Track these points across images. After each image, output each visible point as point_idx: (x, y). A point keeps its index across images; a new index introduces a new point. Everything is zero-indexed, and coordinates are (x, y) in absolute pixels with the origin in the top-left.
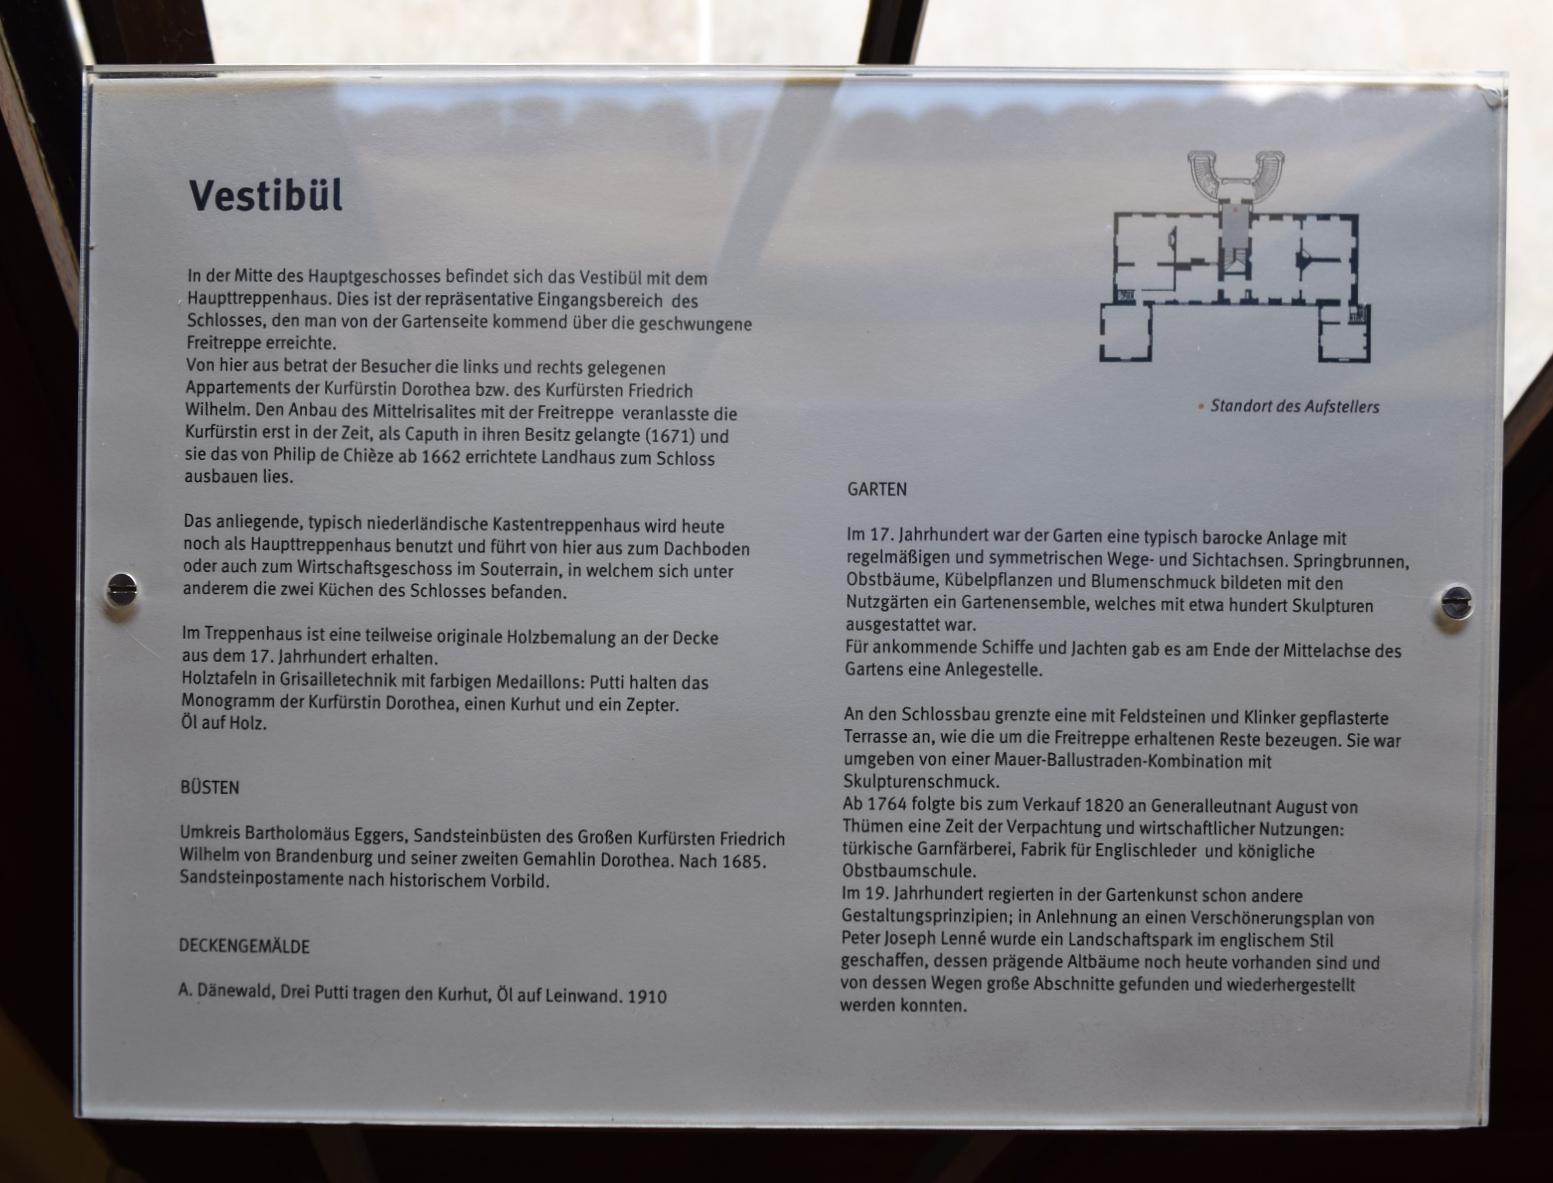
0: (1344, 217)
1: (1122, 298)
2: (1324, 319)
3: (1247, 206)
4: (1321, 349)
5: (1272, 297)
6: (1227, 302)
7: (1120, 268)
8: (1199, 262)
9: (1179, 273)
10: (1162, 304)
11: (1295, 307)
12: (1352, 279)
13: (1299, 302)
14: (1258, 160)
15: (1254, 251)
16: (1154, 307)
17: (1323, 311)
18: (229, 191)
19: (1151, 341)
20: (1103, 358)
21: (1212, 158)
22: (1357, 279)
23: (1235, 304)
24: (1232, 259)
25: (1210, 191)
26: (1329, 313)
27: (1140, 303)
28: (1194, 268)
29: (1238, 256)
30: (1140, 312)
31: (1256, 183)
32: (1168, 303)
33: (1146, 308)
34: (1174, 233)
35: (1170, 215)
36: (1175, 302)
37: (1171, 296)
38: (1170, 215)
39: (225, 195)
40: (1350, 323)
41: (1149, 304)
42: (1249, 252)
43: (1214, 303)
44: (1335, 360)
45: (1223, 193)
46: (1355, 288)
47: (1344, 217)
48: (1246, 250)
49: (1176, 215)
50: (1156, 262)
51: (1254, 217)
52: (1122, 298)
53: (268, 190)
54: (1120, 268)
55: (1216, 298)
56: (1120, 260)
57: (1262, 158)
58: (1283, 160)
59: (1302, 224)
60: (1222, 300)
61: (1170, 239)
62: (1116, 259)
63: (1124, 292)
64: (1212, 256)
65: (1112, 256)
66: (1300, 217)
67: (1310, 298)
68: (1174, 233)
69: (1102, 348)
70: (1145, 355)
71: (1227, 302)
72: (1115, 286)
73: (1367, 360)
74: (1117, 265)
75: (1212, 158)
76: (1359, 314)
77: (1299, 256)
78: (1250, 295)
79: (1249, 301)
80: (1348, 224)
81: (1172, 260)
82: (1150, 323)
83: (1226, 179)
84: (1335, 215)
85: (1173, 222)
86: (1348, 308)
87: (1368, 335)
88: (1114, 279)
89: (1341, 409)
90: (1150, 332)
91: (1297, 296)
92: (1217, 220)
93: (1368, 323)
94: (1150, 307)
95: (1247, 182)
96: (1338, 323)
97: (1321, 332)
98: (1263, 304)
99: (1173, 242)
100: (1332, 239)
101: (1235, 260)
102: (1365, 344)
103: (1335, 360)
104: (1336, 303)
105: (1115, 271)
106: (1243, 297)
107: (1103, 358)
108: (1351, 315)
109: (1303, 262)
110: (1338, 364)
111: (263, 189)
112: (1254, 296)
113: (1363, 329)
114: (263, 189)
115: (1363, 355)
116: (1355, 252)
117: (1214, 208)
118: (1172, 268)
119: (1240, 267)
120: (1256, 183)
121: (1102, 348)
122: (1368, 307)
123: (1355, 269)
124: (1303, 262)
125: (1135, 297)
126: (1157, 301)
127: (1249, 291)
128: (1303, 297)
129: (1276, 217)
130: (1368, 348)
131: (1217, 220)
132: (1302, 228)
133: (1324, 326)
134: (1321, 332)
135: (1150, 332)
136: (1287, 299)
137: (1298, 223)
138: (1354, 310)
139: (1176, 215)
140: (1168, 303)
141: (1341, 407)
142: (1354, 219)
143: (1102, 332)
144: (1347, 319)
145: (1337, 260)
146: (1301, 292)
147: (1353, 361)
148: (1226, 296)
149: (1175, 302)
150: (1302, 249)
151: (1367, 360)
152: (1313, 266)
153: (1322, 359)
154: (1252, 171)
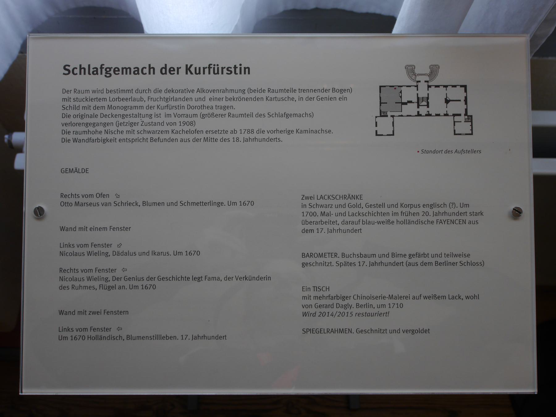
0: (461, 86)
2: (455, 120)
4: (455, 131)
6: (421, 115)
7: (382, 104)
8: (410, 102)
9: (402, 105)
10: (397, 116)
11: (445, 117)
13: (446, 115)
16: (394, 117)
18: (173, 68)
20: (377, 135)
21: (413, 67)
22: (467, 107)
24: (422, 101)
27: (389, 116)
31: (429, 75)
32: (399, 116)
36: (402, 116)
37: (400, 114)
40: (465, 122)
41: (393, 116)
42: (428, 98)
43: (416, 116)
45: (418, 78)
46: (466, 110)
47: (461, 86)
51: (429, 87)
52: (383, 114)
53: (237, 68)
54: (382, 104)
55: (417, 114)
58: (439, 68)
59: (446, 88)
60: (419, 115)
63: (384, 112)
66: (446, 86)
67: (450, 113)
68: (401, 92)
69: (376, 131)
71: (421, 115)
72: (380, 110)
73: (472, 134)
74: (381, 103)
77: (446, 99)
79: (429, 115)
80: (463, 88)
83: (419, 74)
84: (458, 85)
86: (464, 117)
87: (472, 125)
90: (393, 126)
91: (446, 113)
92: (416, 88)
93: (472, 122)
94: (393, 117)
95: (427, 75)
96: (461, 122)
97: (454, 125)
99: (400, 95)
100: (459, 93)
101: (423, 101)
102: (471, 129)
104: (460, 115)
105: (380, 105)
107: (377, 135)
109: (447, 101)
111: (235, 67)
112: (430, 113)
116: (466, 98)
117: (415, 84)
120: (429, 75)
121: (376, 131)
122: (471, 116)
123: (466, 103)
124: (447, 101)
125: (388, 114)
126: (395, 115)
127: (429, 112)
128: (448, 113)
129: (436, 86)
130: (472, 130)
131: (416, 88)
134: (454, 125)
135: (393, 126)
136: (442, 114)
137: (445, 88)
138: (466, 117)
140: (399, 116)
142: (465, 87)
143: (376, 126)
145: (460, 101)
146: (447, 111)
147: (466, 134)
148: (420, 113)
149: (402, 116)
150: (447, 97)
151: (472, 134)
152: (451, 102)
153: (455, 134)
154: (428, 71)
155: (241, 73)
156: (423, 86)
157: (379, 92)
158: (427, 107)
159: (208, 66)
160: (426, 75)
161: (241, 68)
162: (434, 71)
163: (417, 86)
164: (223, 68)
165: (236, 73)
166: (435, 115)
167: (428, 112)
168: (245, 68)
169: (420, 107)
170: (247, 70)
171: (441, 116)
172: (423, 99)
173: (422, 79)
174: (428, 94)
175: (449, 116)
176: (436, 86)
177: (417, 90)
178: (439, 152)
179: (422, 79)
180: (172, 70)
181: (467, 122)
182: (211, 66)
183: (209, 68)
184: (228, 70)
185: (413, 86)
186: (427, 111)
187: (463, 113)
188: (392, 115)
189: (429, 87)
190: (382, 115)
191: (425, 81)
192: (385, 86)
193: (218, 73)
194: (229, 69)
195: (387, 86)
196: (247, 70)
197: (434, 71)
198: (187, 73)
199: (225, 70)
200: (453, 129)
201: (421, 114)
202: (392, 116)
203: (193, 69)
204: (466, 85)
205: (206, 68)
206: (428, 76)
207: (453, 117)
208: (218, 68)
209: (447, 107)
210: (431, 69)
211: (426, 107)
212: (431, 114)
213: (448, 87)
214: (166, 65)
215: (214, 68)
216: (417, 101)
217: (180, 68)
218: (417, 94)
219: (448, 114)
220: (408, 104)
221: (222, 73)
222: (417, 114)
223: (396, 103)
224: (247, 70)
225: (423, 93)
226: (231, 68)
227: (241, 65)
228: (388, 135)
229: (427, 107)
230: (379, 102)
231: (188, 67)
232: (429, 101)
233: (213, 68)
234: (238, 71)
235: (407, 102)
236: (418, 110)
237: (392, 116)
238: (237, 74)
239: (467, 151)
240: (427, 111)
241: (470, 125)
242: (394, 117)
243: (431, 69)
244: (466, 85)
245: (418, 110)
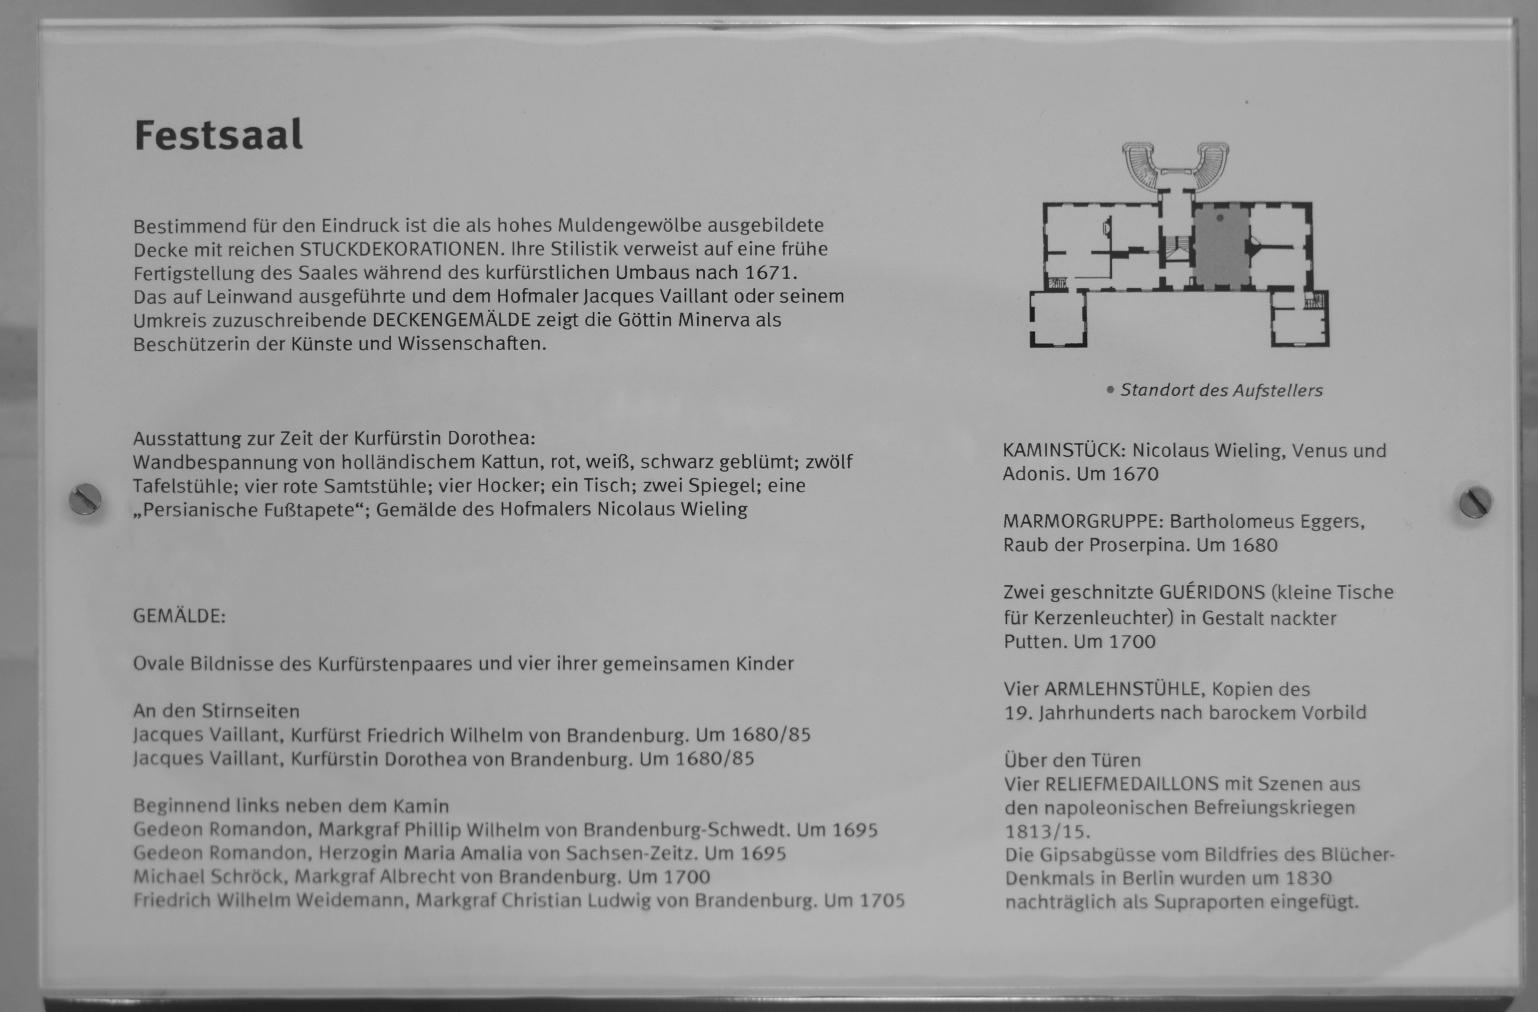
0: (1296, 205)
1: (1053, 286)
2: (1276, 305)
3: (1189, 195)
4: (1273, 335)
5: (1219, 284)
6: (1170, 289)
8: (1139, 250)
9: (1114, 260)
11: (1244, 293)
12: (1307, 265)
14: (1200, 151)
15: (1197, 239)
16: (1088, 294)
17: (1274, 296)
19: (1086, 328)
20: (1033, 344)
22: (1312, 265)
23: (1178, 291)
25: (1147, 180)
26: (1281, 299)
28: (1131, 256)
29: (1180, 244)
30: (1074, 300)
31: (1198, 172)
32: (1103, 290)
34: (1109, 221)
35: (1103, 205)
36: (1112, 290)
37: (1107, 284)
38: (1103, 205)
40: (1305, 309)
41: (1084, 291)
43: (1155, 290)
45: (1162, 183)
46: (1310, 275)
47: (1296, 205)
48: (1190, 238)
49: (1111, 205)
52: (1053, 286)
55: (1157, 286)
56: (1051, 248)
60: (1164, 286)
61: (1104, 230)
62: (1046, 247)
63: (1057, 279)
64: (1152, 244)
65: (1043, 245)
67: (1260, 282)
68: (1109, 221)
69: (1033, 335)
70: (1081, 341)
71: (1170, 289)
72: (1046, 274)
75: (1149, 149)
77: (1248, 243)
79: (1194, 287)
81: (1108, 249)
84: (1285, 203)
85: (1108, 211)
87: (1326, 320)
88: (1045, 267)
91: (1247, 283)
92: (1156, 209)
96: (1293, 309)
97: (1273, 318)
99: (1108, 230)
101: (1177, 247)
104: (1290, 289)
106: (1187, 284)
107: (1033, 344)
110: (1292, 349)
115: (1322, 339)
116: (1309, 239)
118: (1108, 256)
120: (1198, 172)
121: (1033, 335)
122: (1326, 293)
123: (1310, 255)
125: (1068, 285)
128: (1253, 284)
130: (1327, 332)
131: (1156, 209)
134: (1273, 318)
138: (1310, 295)
139: (1111, 205)
140: (1103, 290)
143: (1032, 319)
144: (1303, 305)
145: (1291, 247)
148: (1168, 283)
149: (1112, 290)
152: (1263, 251)
153: (1274, 344)
154: (1194, 161)
163: (1159, 205)
173: (1177, 182)
178: (1182, 391)
179: (1177, 182)
181: (1311, 309)
185: (1148, 203)
187: (1300, 282)
189: (1196, 206)
190: (1050, 286)
191: (1186, 191)
195: (1067, 203)
200: (1270, 330)
201: (1172, 287)
202: (1080, 291)
207: (1269, 294)
211: (1188, 264)
212: (1203, 286)
216: (1158, 249)
218: (1161, 228)
220: (1131, 256)
222: (1157, 286)
223: (1093, 252)
228: (1067, 346)
232: (1194, 246)
236: (1162, 273)
237: (1080, 291)
245: (1162, 273)
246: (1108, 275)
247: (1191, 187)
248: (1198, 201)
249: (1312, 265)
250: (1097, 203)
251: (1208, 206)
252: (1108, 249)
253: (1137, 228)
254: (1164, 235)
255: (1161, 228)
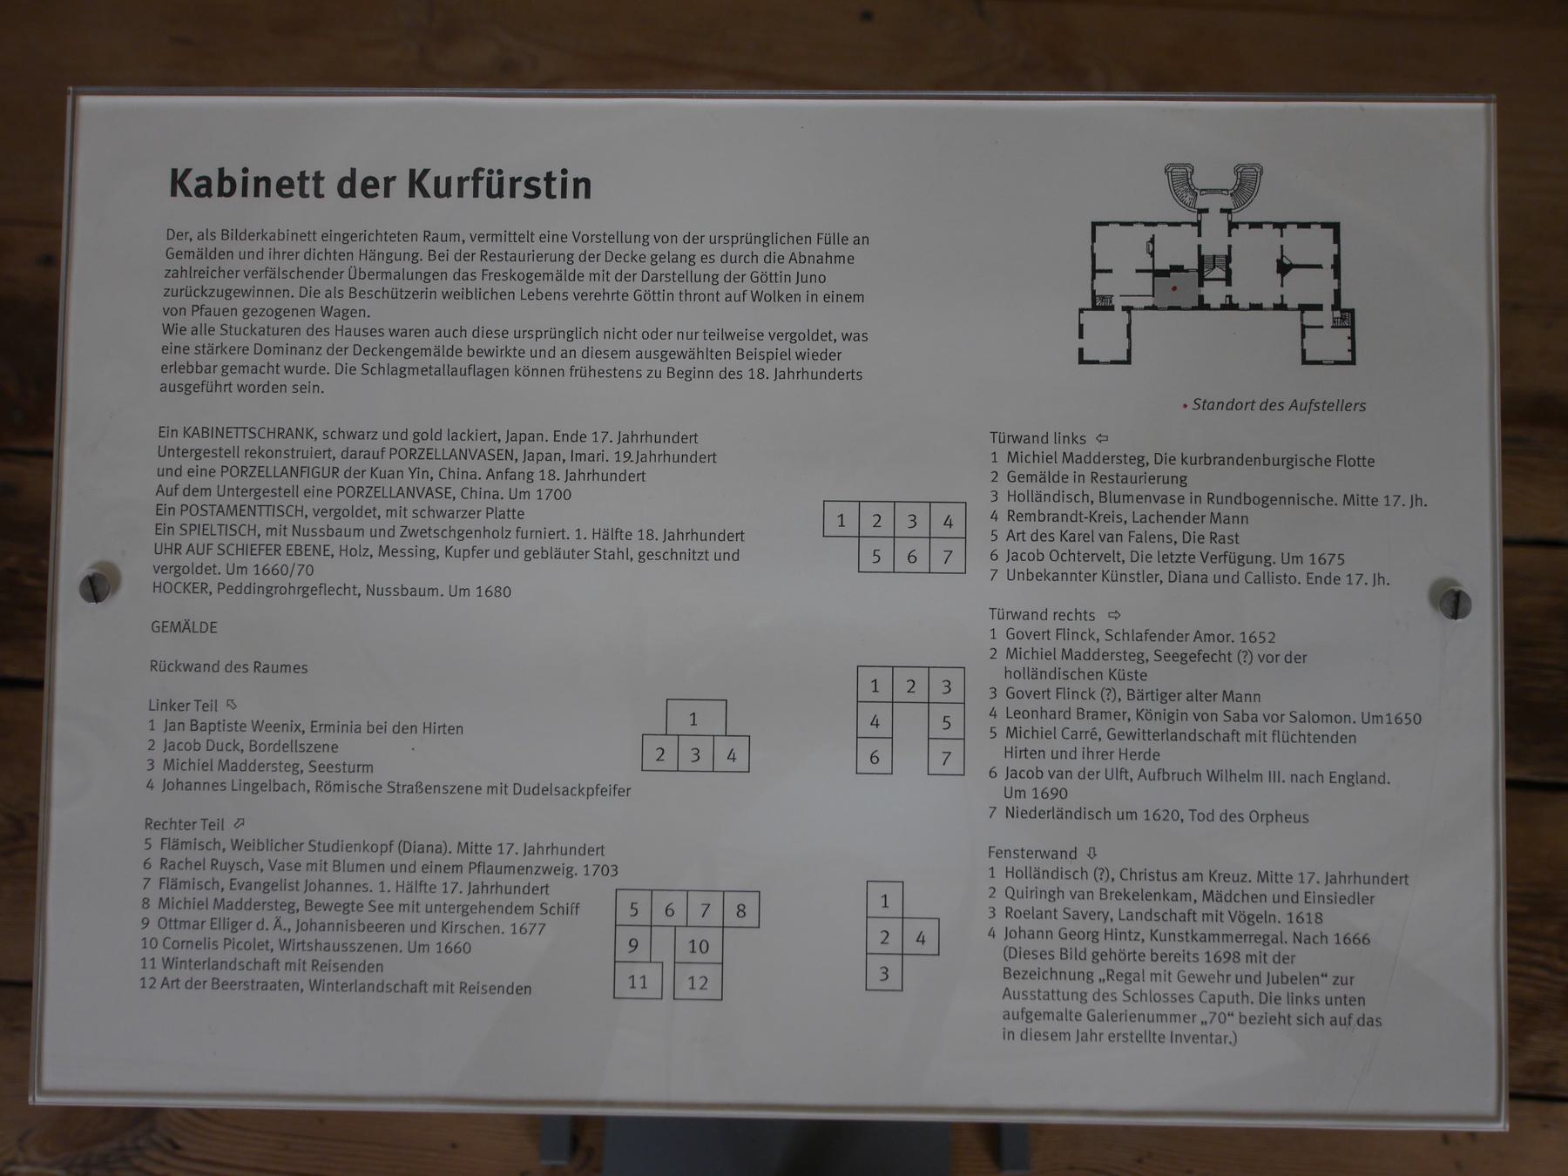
0: (1325, 225)
2: (1305, 323)
4: (1304, 352)
6: (1208, 307)
7: (1097, 274)
8: (1178, 269)
9: (1156, 278)
10: (1140, 309)
13: (1281, 307)
14: (1236, 172)
16: (1132, 312)
20: (1082, 361)
21: (1189, 170)
22: (1339, 284)
25: (1188, 202)
26: (1311, 317)
27: (1118, 308)
32: (1146, 308)
33: (1125, 312)
34: (1152, 241)
35: (1147, 224)
36: (1154, 308)
38: (1147, 224)
39: (370, 183)
40: (1333, 327)
41: (1128, 309)
42: (1228, 259)
44: (1320, 363)
45: (1201, 204)
46: (1337, 294)
47: (1325, 225)
49: (1154, 224)
50: (1134, 269)
51: (1233, 225)
52: (1100, 304)
54: (1097, 274)
56: (1097, 268)
57: (1240, 170)
60: (1202, 306)
63: (1103, 297)
66: (1280, 226)
67: (1292, 302)
68: (1152, 241)
69: (1081, 351)
71: (1208, 307)
72: (1093, 292)
73: (1353, 362)
74: (1094, 271)
76: (1343, 318)
77: (1280, 262)
78: (1230, 300)
79: (1230, 306)
81: (1151, 268)
82: (1129, 326)
87: (1352, 338)
88: (1092, 285)
89: (1325, 408)
91: (1280, 302)
92: (1197, 228)
93: (1352, 327)
94: (1129, 313)
97: (1303, 336)
98: (1243, 310)
99: (1151, 249)
100: (1317, 246)
103: (1320, 363)
104: (1319, 307)
105: (1093, 278)
107: (1082, 361)
108: (1334, 318)
109: (1283, 268)
111: (549, 178)
112: (1234, 301)
113: (1348, 332)
114: (549, 178)
115: (1348, 357)
116: (1337, 258)
117: (1193, 218)
118: (1151, 274)
119: (1219, 273)
120: (1234, 194)
121: (1081, 351)
122: (1352, 311)
123: (1337, 275)
124: (1283, 268)
125: (1113, 303)
127: (1230, 297)
128: (1285, 302)
129: (1253, 225)
130: (1353, 350)
132: (1282, 236)
133: (1306, 329)
134: (1303, 336)
136: (1268, 304)
137: (1278, 231)
138: (1337, 314)
139: (1154, 224)
140: (1146, 308)
141: (1326, 406)
142: (1335, 227)
143: (1081, 336)
145: (1319, 266)
146: (1282, 296)
147: (1337, 363)
148: (1205, 302)
150: (1282, 256)
151: (1353, 362)
153: (1305, 362)
154: (1230, 181)
155: (564, 195)
156: (1215, 224)
157: (1090, 240)
158: (1227, 285)
159: (472, 175)
160: (1224, 192)
161: (564, 181)
162: (1246, 183)
163: (1198, 224)
164: (513, 181)
165: (549, 195)
166: (1248, 307)
167: (1228, 299)
168: (577, 182)
169: (1205, 282)
170: (582, 186)
171: (1266, 309)
172: (1214, 260)
174: (1230, 247)
175: (1239, 310)
176: (1253, 225)
177: (1199, 235)
179: (1215, 203)
180: (369, 186)
181: (1340, 327)
182: (481, 174)
183: (476, 179)
184: (528, 185)
186: (1227, 296)
187: (1328, 301)
188: (1125, 305)
189: (1233, 225)
191: (1223, 211)
192: (1106, 224)
193: (500, 194)
194: (533, 183)
196: (583, 186)
197: (1246, 183)
198: (412, 194)
199: (521, 188)
200: (1300, 347)
201: (1209, 305)
202: (1124, 308)
203: (428, 183)
204: (1339, 223)
205: (467, 178)
206: (1231, 195)
208: (501, 181)
209: (1282, 286)
210: (1239, 174)
211: (1224, 282)
212: (1238, 304)
213: (1285, 228)
214: (353, 171)
215: (489, 180)
216: (1197, 268)
217: (394, 178)
218: (1199, 247)
219: (1286, 305)
221: (513, 195)
223: (1138, 271)
224: (582, 186)
225: (1215, 243)
226: (537, 180)
227: (564, 171)
228: (1113, 362)
229: (1227, 285)
230: (1090, 268)
231: (417, 177)
232: (1231, 266)
233: (485, 180)
234: (556, 188)
235: (1169, 268)
237: (1124, 308)
238: (555, 197)
239: (1326, 406)
240: (1227, 296)
241: (1349, 338)
242: (1132, 312)
243: (1239, 174)
244: (1339, 223)
246: (1151, 294)
247: (1229, 208)
248: (1233, 221)
249: (1339, 284)
250: (1141, 223)
251: (1243, 225)
252: (1151, 268)
253: (1178, 248)
254: (1203, 253)
255: (1199, 247)
